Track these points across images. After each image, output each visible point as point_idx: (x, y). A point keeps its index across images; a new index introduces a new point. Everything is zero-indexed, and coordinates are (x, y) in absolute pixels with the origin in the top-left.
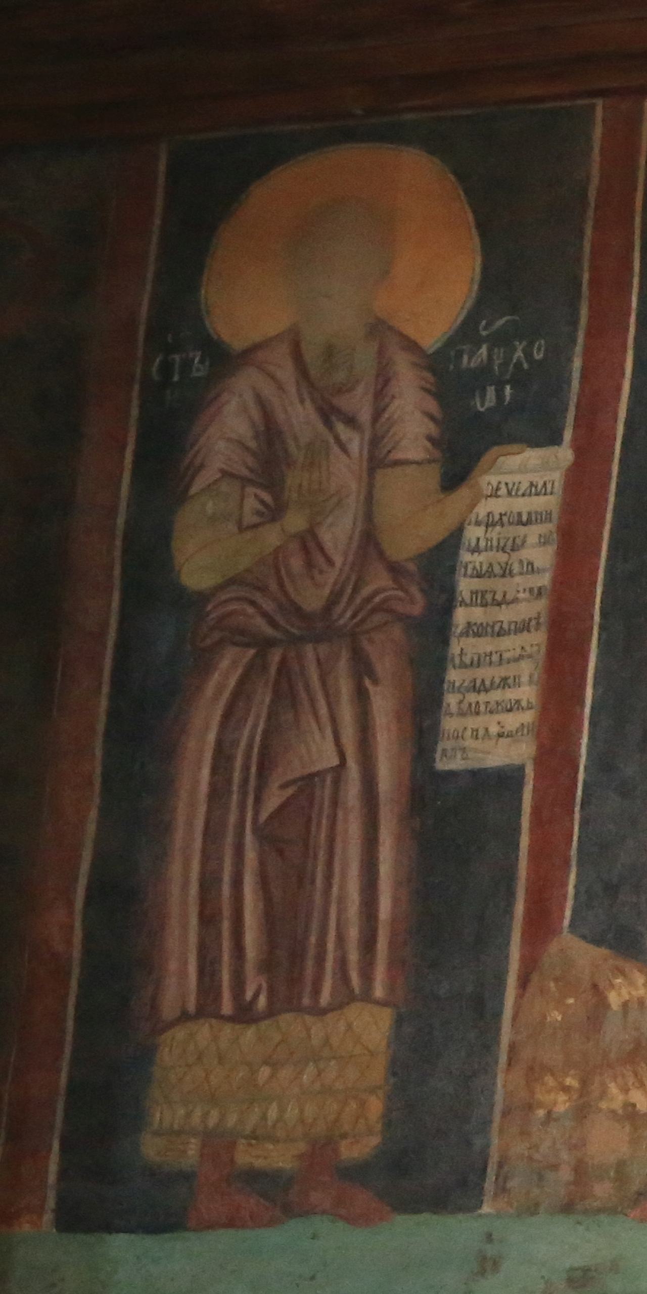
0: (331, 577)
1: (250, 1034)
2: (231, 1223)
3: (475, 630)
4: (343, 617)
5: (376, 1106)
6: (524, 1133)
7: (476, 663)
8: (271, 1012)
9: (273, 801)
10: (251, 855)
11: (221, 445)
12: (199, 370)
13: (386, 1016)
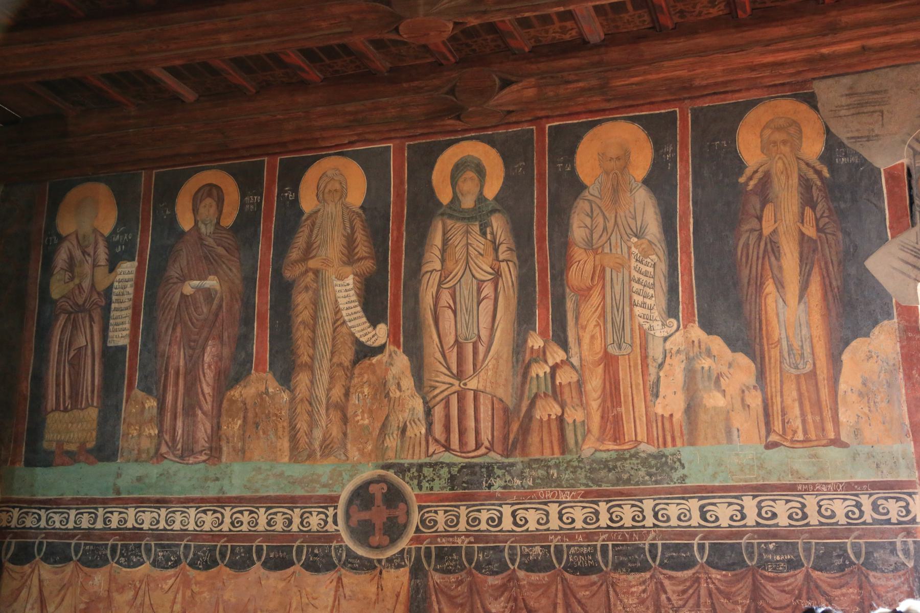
0: (84, 296)
1: (67, 415)
2: (63, 465)
3: (116, 309)
4: (87, 306)
5: (94, 434)
6: (127, 441)
7: (116, 318)
8: (72, 409)
9: (72, 354)
10: (67, 368)
11: (61, 261)
12: (56, 242)
13: (97, 410)
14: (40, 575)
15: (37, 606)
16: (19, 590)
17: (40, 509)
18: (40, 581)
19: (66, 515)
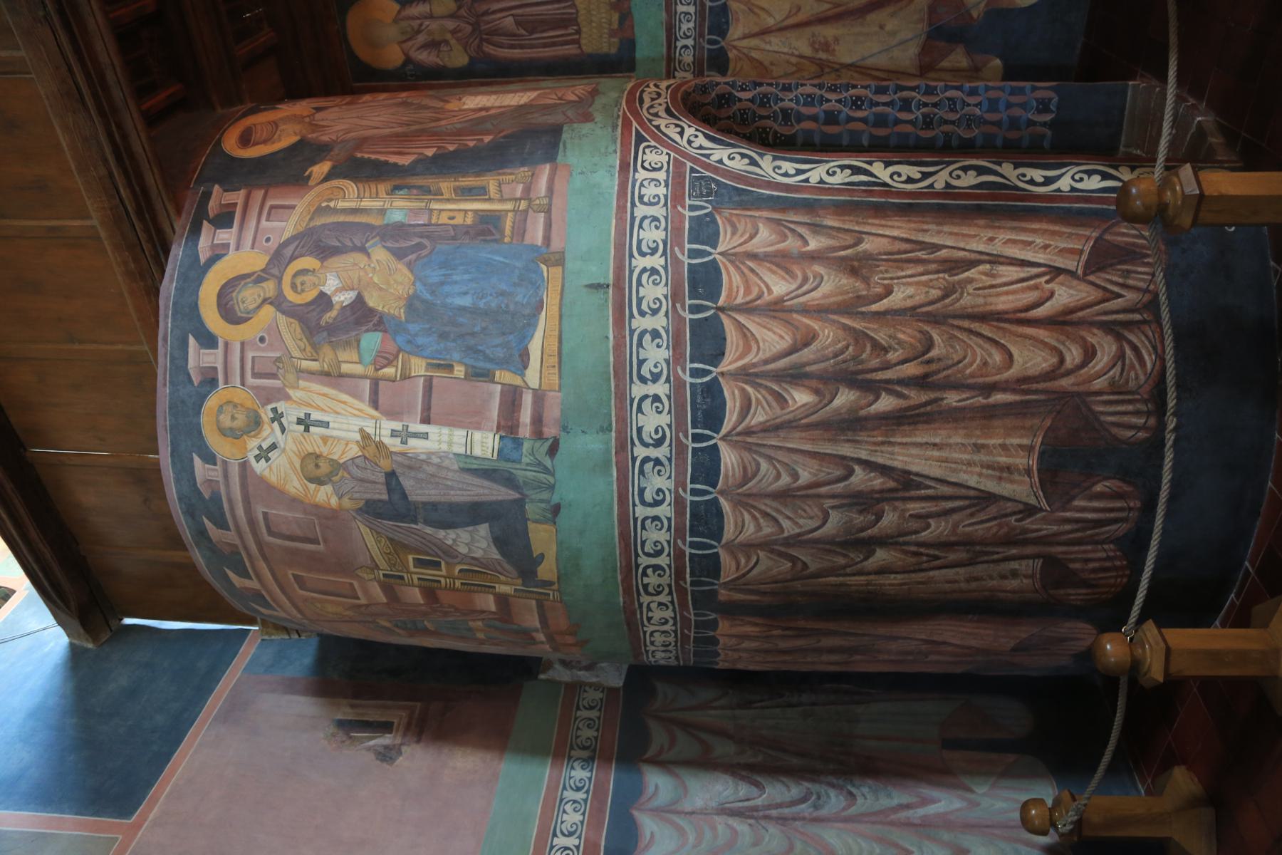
0: (463, 25)
1: (584, 30)
2: (633, 28)
4: (472, 20)
8: (578, 25)
9: (523, 32)
12: (411, 67)
14: (739, 39)
15: (767, 38)
16: (751, 59)
17: (676, 47)
18: (745, 37)
19: (683, 15)
